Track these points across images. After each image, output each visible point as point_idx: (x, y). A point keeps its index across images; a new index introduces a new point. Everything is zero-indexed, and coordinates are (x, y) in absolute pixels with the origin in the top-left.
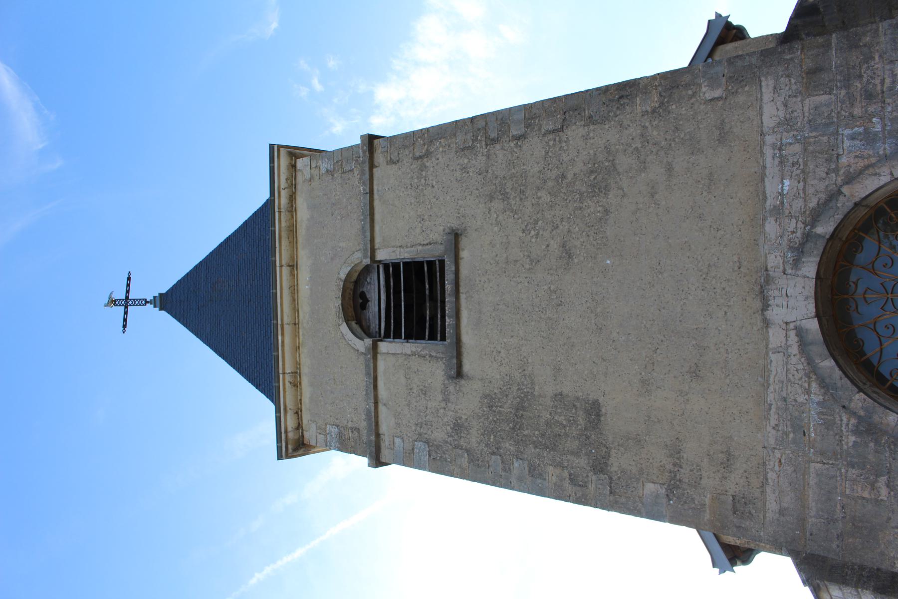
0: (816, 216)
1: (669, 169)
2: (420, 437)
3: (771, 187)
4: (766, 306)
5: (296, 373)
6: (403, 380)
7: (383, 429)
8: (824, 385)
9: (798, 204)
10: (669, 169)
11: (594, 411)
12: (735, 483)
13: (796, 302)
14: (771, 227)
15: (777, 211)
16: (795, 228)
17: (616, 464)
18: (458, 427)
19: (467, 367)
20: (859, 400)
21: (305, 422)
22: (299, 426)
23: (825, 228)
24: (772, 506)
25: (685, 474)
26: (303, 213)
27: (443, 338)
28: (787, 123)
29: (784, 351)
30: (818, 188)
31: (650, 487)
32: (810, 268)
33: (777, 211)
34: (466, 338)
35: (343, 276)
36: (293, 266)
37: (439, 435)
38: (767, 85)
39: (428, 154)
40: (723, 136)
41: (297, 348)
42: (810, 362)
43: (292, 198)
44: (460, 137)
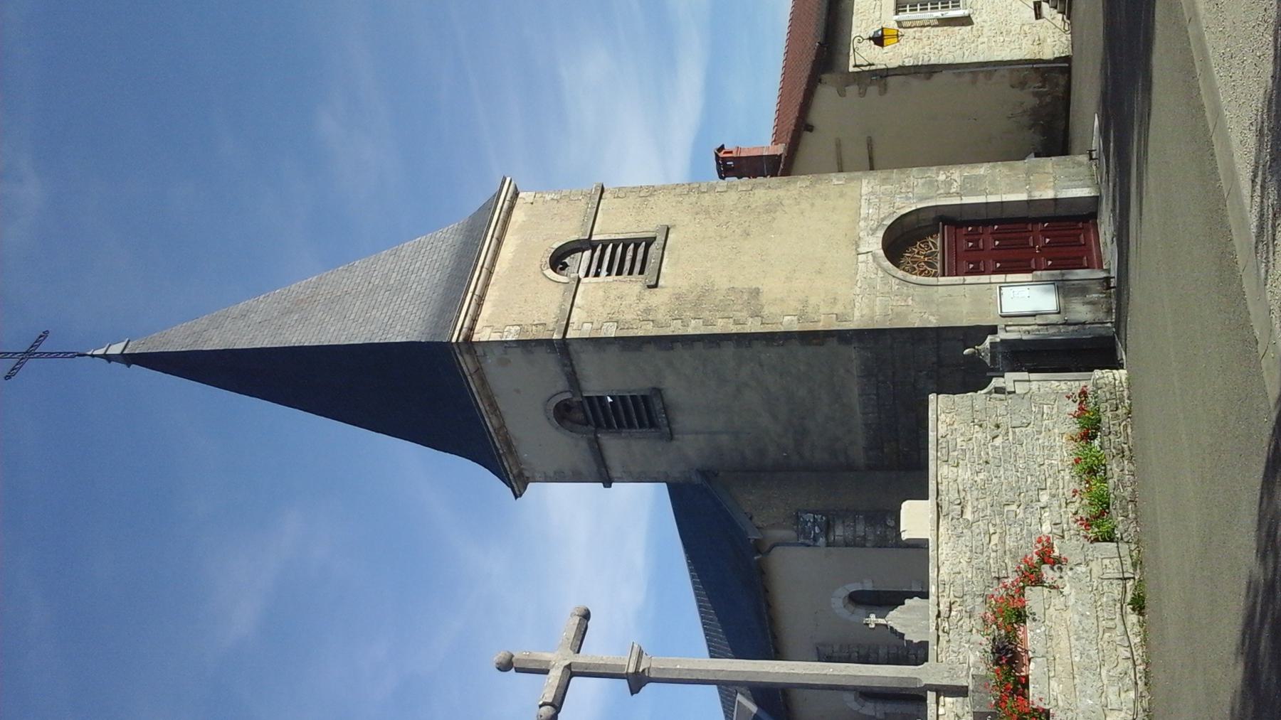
0: (883, 219)
1: (813, 205)
2: (611, 320)
3: (864, 212)
4: (858, 246)
5: (481, 299)
6: (601, 293)
7: (573, 319)
8: (885, 270)
9: (875, 217)
10: (813, 205)
11: (756, 292)
12: (838, 309)
13: (874, 244)
14: (862, 224)
15: (866, 219)
16: (874, 224)
17: (766, 312)
18: (647, 311)
19: (661, 282)
20: (900, 273)
21: (477, 328)
22: (472, 329)
23: (888, 222)
24: (857, 314)
25: (810, 309)
26: (518, 216)
27: (641, 272)
28: (872, 193)
29: (866, 262)
30: (885, 210)
31: (787, 318)
32: (880, 234)
33: (866, 219)
34: (663, 270)
35: (556, 246)
36: (500, 242)
37: (628, 317)
38: (865, 182)
39: (651, 195)
40: (842, 195)
41: (486, 285)
42: (879, 265)
43: (511, 208)
44: (678, 190)
